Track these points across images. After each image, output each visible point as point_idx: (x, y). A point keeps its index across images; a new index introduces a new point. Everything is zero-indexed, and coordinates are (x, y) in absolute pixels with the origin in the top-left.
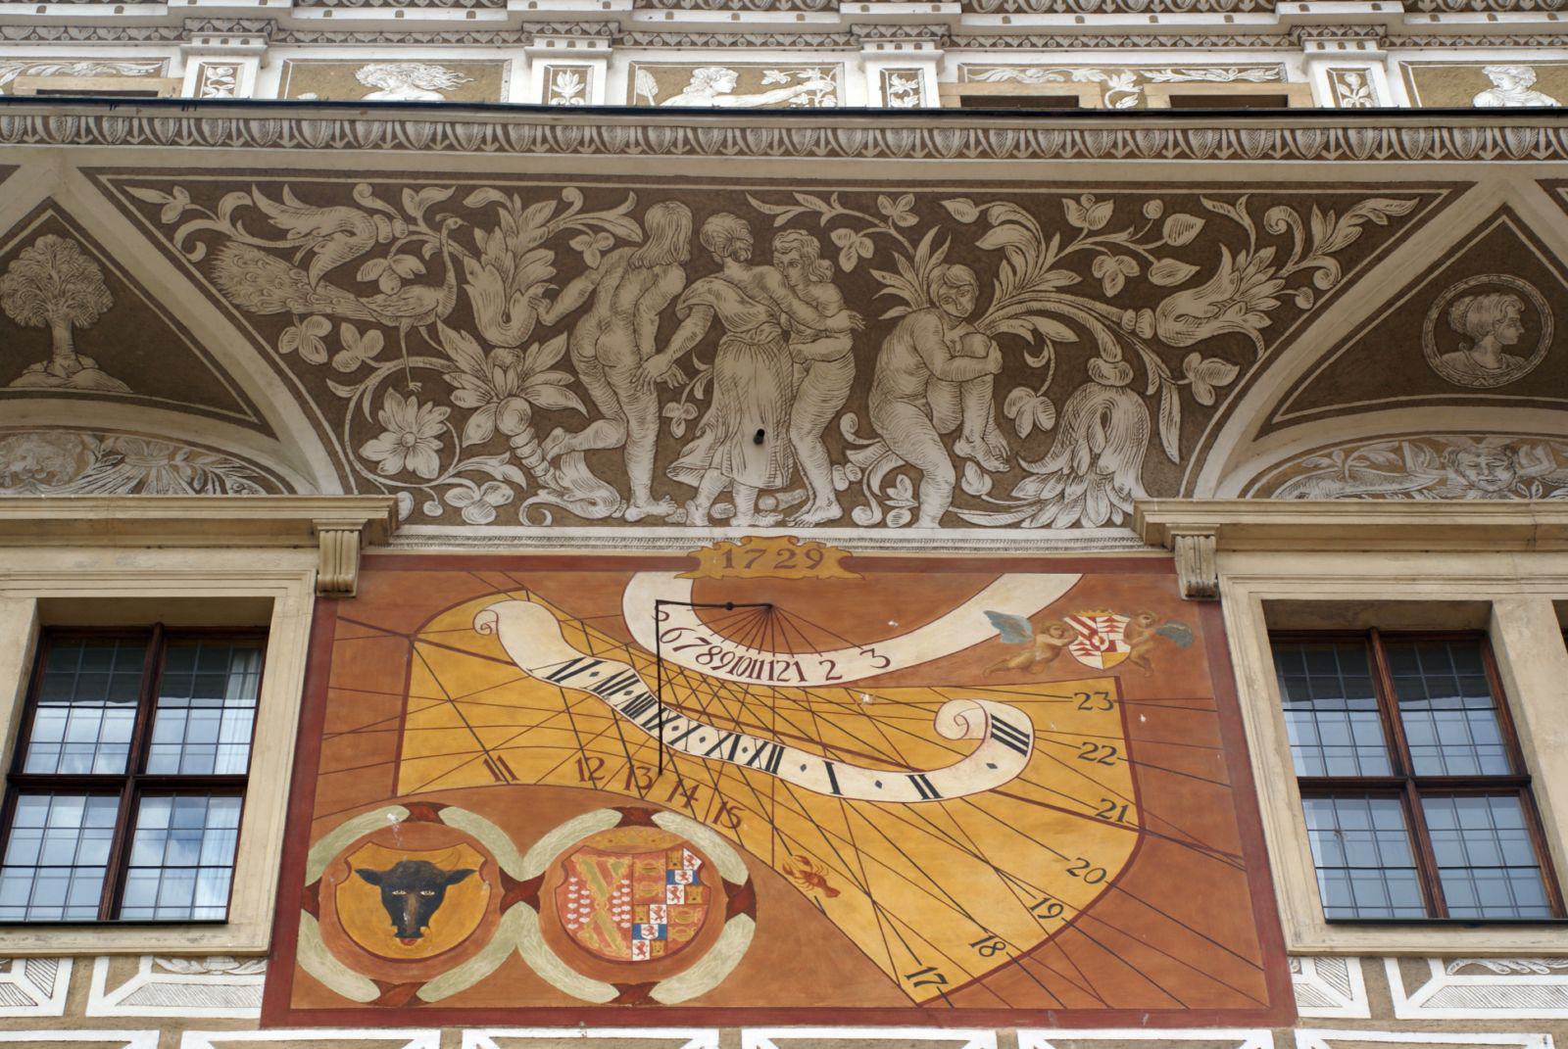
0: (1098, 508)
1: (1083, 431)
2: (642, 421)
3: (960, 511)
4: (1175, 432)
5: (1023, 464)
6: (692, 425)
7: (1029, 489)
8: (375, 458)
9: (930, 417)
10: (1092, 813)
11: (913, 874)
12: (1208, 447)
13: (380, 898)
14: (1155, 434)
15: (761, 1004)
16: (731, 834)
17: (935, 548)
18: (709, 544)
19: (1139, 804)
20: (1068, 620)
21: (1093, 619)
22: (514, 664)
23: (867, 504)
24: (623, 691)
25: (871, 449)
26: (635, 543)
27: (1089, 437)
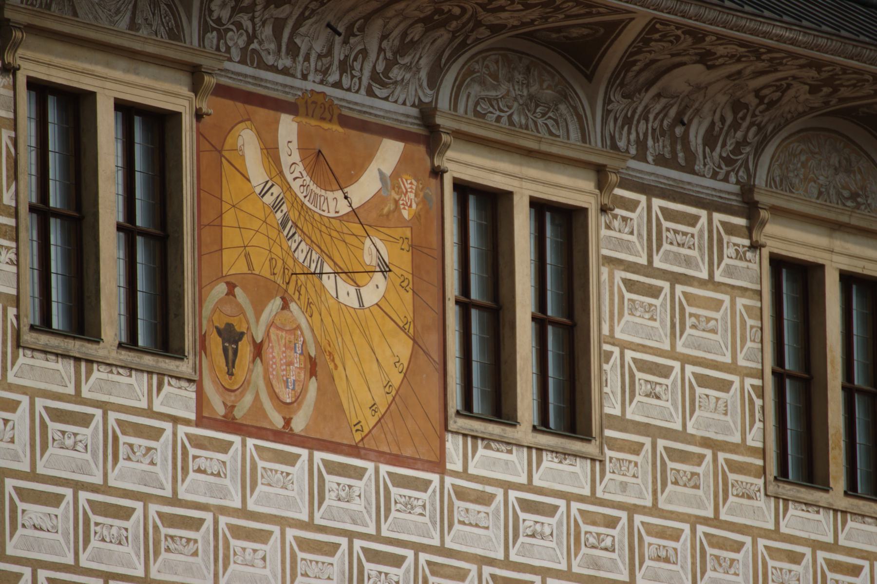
0: (411, 93)
1: (423, 45)
2: (299, 8)
3: (374, 84)
4: (450, 51)
5: (398, 57)
6: (313, 11)
7: (396, 73)
8: (213, 9)
9: (385, 26)
10: (401, 325)
11: (356, 359)
12: (454, 61)
13: (221, 347)
14: (444, 51)
15: (318, 436)
16: (309, 319)
17: (360, 111)
18: (300, 93)
19: (414, 321)
20: (400, 180)
21: (406, 180)
22: (249, 180)
23: (347, 73)
24: (280, 211)
25: (358, 37)
26: (280, 88)
27: (424, 48)
